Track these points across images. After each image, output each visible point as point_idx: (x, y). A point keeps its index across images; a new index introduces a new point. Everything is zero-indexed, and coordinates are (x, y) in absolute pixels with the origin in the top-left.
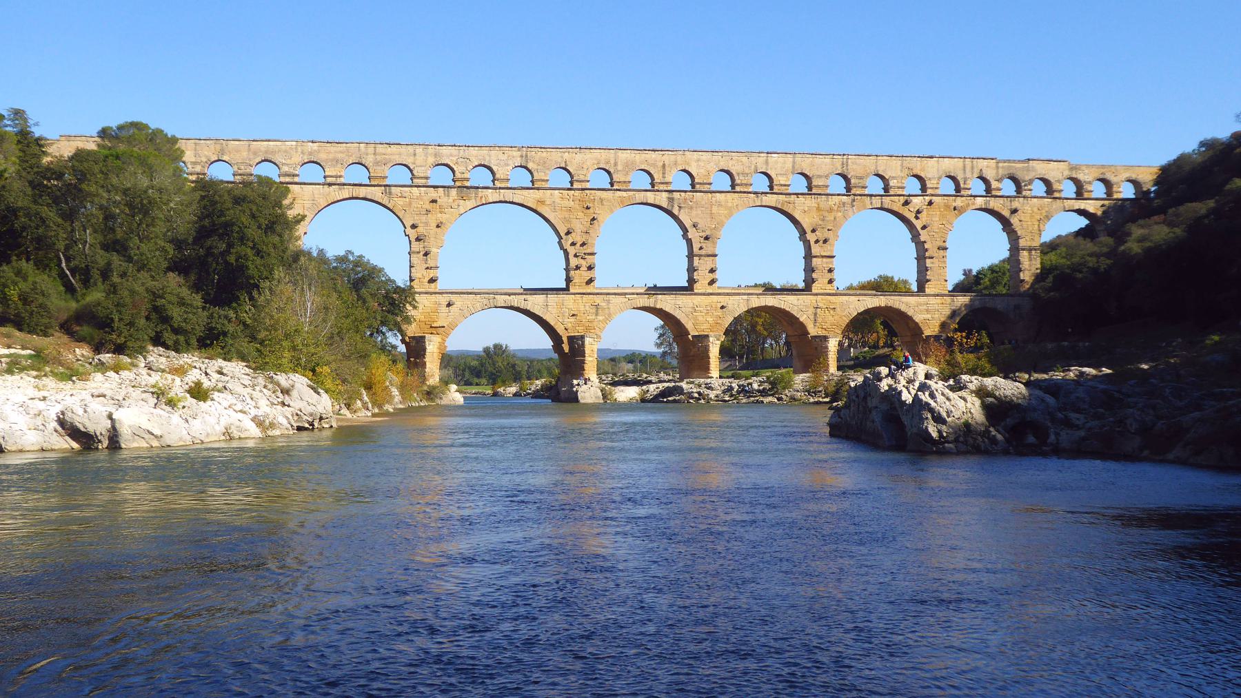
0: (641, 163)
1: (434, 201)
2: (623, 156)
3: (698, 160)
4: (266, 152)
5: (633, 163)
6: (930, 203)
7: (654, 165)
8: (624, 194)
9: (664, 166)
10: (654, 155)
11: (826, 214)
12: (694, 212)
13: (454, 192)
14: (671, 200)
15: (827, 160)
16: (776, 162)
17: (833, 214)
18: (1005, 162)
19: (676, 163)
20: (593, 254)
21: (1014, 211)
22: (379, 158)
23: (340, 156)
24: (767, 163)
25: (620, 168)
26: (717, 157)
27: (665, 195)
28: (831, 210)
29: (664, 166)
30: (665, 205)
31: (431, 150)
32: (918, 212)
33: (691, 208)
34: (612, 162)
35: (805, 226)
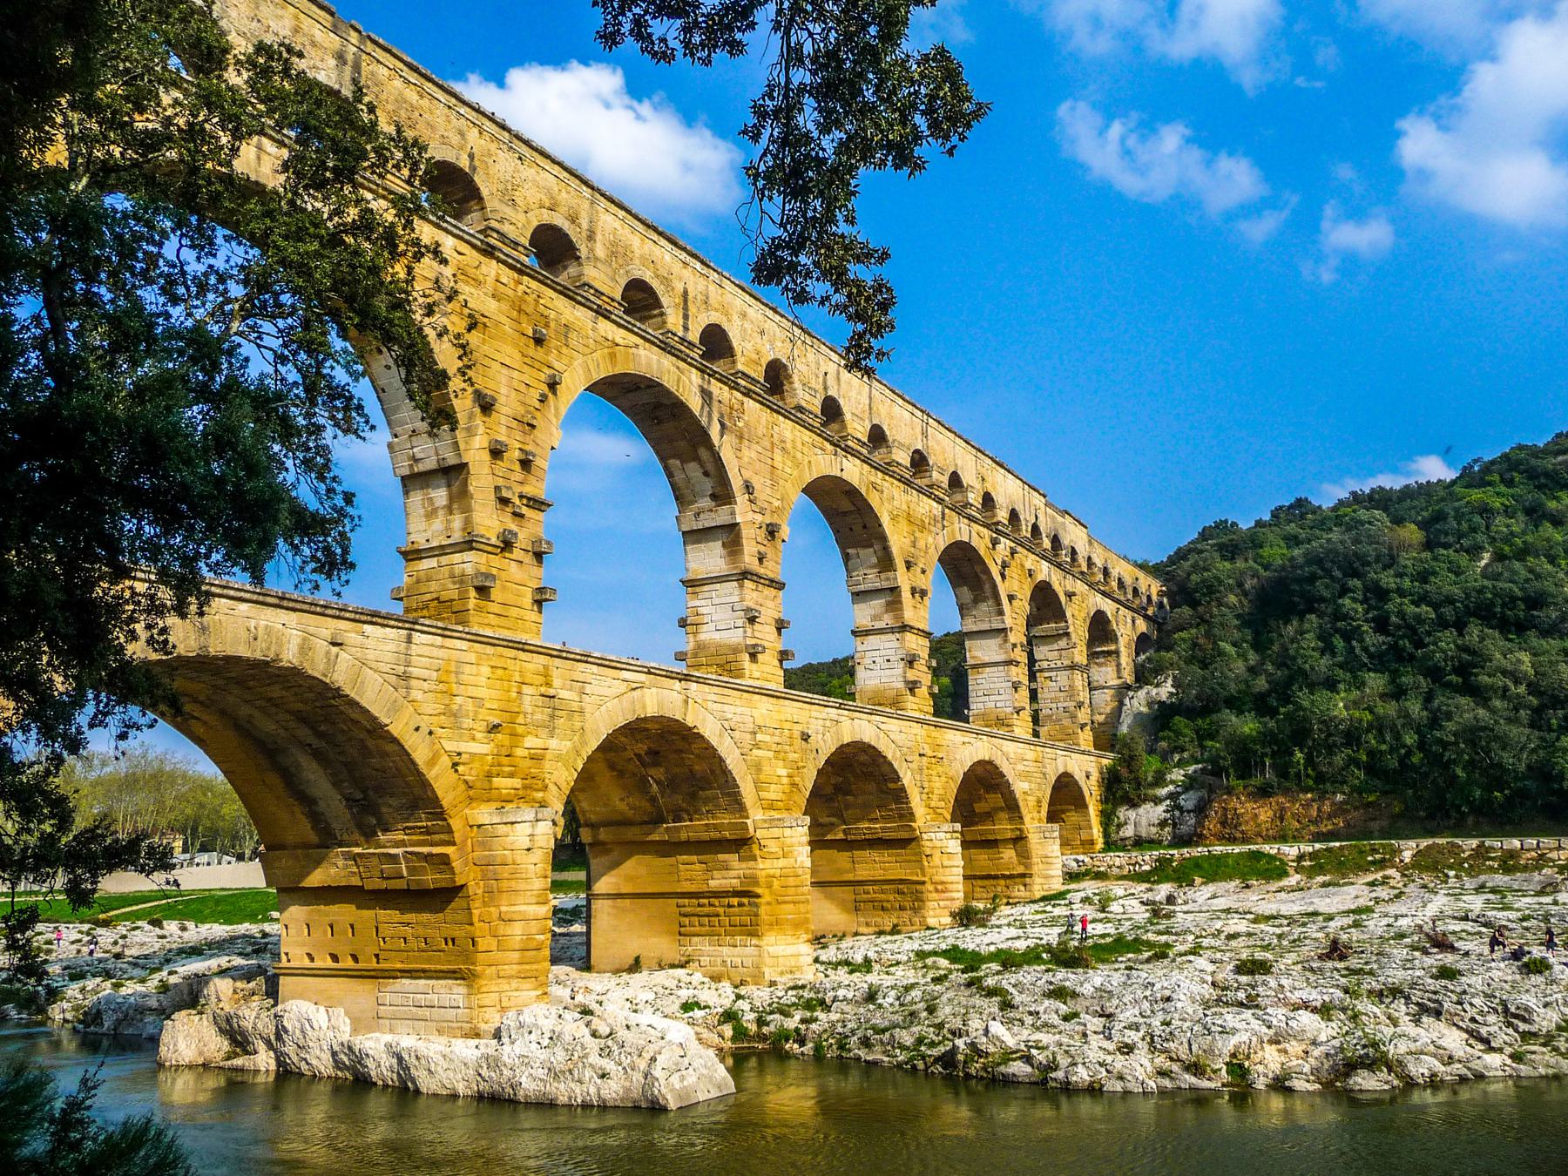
6: (1013, 552)
8: (620, 335)
11: (918, 534)
12: (745, 451)
14: (706, 395)
20: (538, 504)
21: (1070, 595)
27: (695, 376)
29: (685, 293)
32: (1005, 565)
34: (585, 226)
35: (895, 550)
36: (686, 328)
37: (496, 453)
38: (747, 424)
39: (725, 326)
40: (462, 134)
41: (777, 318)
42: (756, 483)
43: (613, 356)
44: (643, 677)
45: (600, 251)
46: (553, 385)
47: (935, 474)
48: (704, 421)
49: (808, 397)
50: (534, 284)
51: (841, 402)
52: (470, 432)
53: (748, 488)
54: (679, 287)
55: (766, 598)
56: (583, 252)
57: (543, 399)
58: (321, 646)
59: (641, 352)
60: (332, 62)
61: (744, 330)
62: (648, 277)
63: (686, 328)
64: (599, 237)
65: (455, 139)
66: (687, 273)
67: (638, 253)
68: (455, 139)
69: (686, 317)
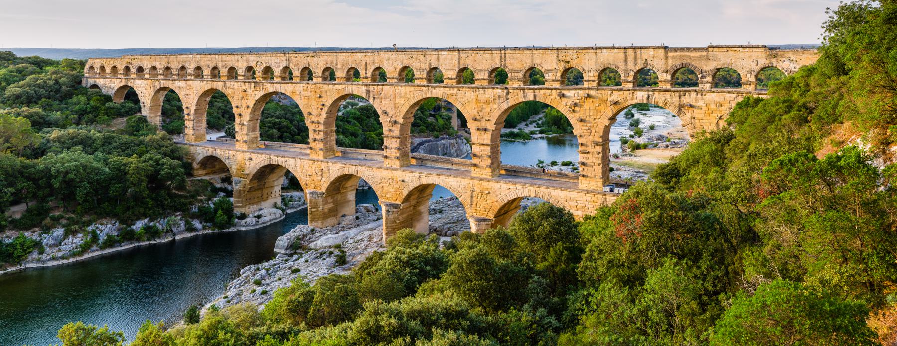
1: (245, 91)
2: (342, 57)
8: (340, 87)
9: (366, 64)
14: (368, 92)
15: (488, 55)
16: (445, 59)
17: (491, 105)
18: (676, 50)
24: (438, 59)
25: (339, 66)
26: (401, 56)
27: (364, 88)
28: (488, 102)
29: (366, 64)
30: (364, 95)
47: (509, 75)
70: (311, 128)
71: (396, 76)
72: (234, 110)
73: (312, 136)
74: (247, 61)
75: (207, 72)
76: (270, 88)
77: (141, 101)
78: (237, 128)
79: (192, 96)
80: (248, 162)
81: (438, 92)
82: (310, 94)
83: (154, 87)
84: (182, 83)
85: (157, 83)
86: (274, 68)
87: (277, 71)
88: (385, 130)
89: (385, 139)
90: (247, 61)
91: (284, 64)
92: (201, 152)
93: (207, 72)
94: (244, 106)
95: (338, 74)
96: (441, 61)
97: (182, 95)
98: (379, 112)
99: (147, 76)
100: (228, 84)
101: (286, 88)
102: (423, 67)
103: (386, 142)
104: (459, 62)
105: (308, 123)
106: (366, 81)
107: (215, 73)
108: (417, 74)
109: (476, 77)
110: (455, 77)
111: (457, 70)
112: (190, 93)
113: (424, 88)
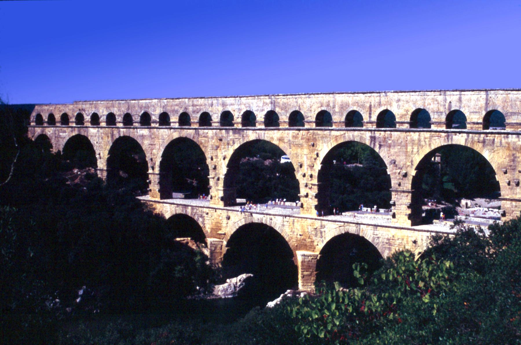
0: (353, 104)
3: (399, 100)
4: (145, 107)
5: (348, 105)
7: (363, 106)
9: (370, 106)
10: (361, 97)
12: (393, 151)
13: (231, 132)
14: (373, 139)
16: (470, 100)
19: (380, 104)
22: (195, 108)
23: (176, 108)
24: (460, 100)
25: (337, 109)
27: (368, 134)
31: (221, 100)
33: (390, 146)
36: (370, 117)
37: (304, 176)
38: (393, 141)
39: (389, 109)
40: (297, 102)
41: (417, 93)
42: (398, 159)
43: (336, 140)
44: (343, 224)
45: (337, 109)
46: (317, 155)
48: (372, 146)
49: (436, 116)
50: (311, 131)
51: (462, 110)
52: (298, 171)
53: (394, 162)
54: (368, 105)
55: (402, 196)
56: (331, 112)
57: (315, 159)
58: (268, 220)
59: (346, 135)
60: (270, 105)
61: (399, 106)
62: (355, 108)
63: (370, 117)
64: (337, 106)
65: (295, 104)
66: (370, 99)
67: (350, 103)
68: (295, 104)
69: (370, 114)
70: (302, 182)
71: (408, 120)
72: (208, 161)
73: (303, 191)
74: (224, 105)
75: (174, 119)
76: (251, 135)
77: (97, 152)
78: (212, 183)
79: (157, 147)
80: (225, 221)
81: (460, 139)
82: (301, 142)
83: (112, 135)
84: (145, 132)
85: (116, 132)
86: (256, 113)
87: (260, 117)
88: (394, 183)
89: (393, 193)
90: (224, 105)
91: (269, 108)
92: (167, 209)
93: (174, 119)
94: (220, 156)
95: (336, 118)
96: (464, 102)
97: (145, 144)
98: (387, 161)
99: (58, 125)
100: (201, 132)
101: (272, 136)
102: (442, 109)
103: (394, 197)
104: (487, 104)
105: (298, 176)
106: (370, 127)
107: (184, 120)
108: (434, 118)
109: (508, 121)
110: (481, 121)
111: (484, 113)
112: (155, 144)
113: (443, 134)
